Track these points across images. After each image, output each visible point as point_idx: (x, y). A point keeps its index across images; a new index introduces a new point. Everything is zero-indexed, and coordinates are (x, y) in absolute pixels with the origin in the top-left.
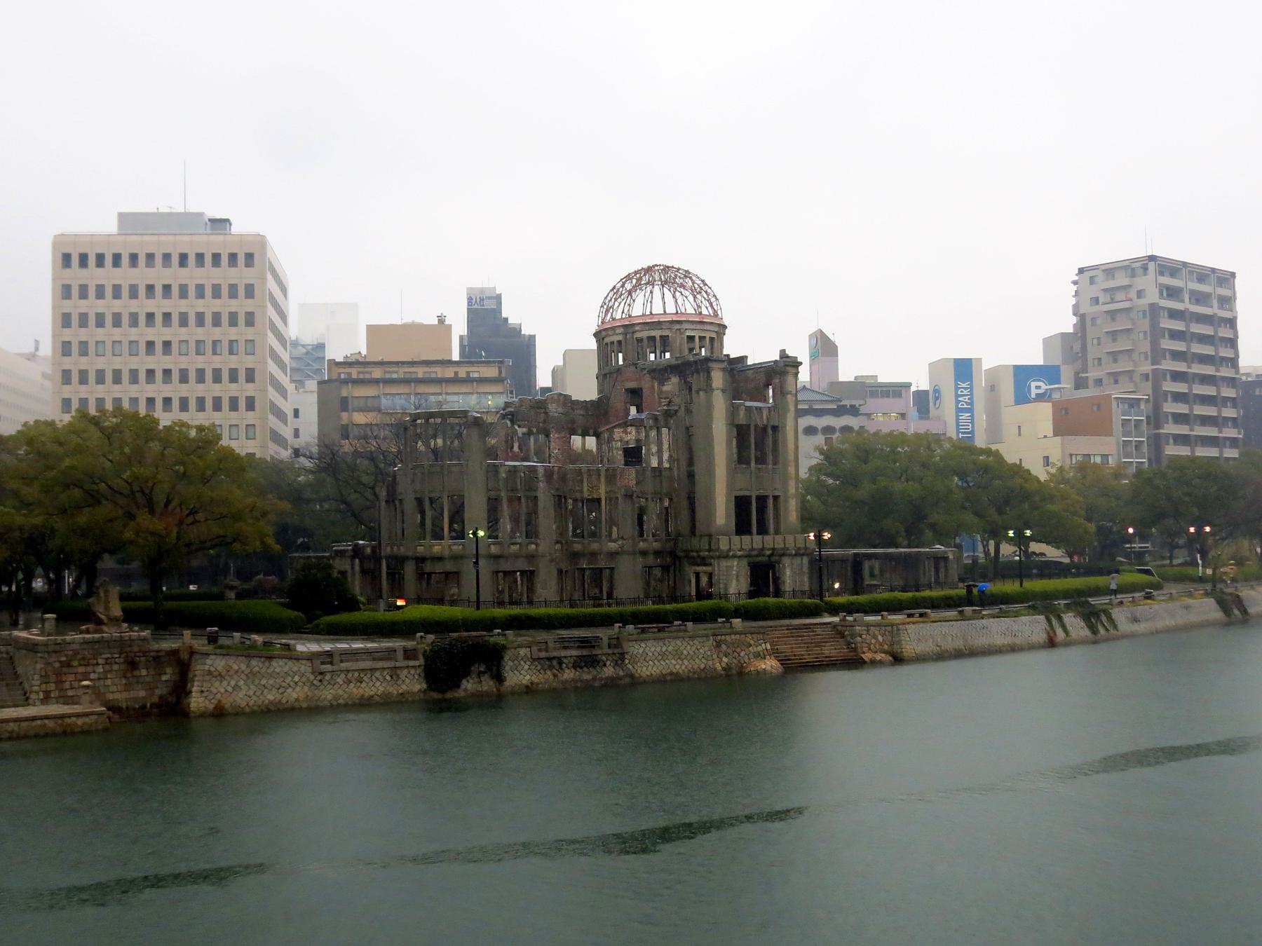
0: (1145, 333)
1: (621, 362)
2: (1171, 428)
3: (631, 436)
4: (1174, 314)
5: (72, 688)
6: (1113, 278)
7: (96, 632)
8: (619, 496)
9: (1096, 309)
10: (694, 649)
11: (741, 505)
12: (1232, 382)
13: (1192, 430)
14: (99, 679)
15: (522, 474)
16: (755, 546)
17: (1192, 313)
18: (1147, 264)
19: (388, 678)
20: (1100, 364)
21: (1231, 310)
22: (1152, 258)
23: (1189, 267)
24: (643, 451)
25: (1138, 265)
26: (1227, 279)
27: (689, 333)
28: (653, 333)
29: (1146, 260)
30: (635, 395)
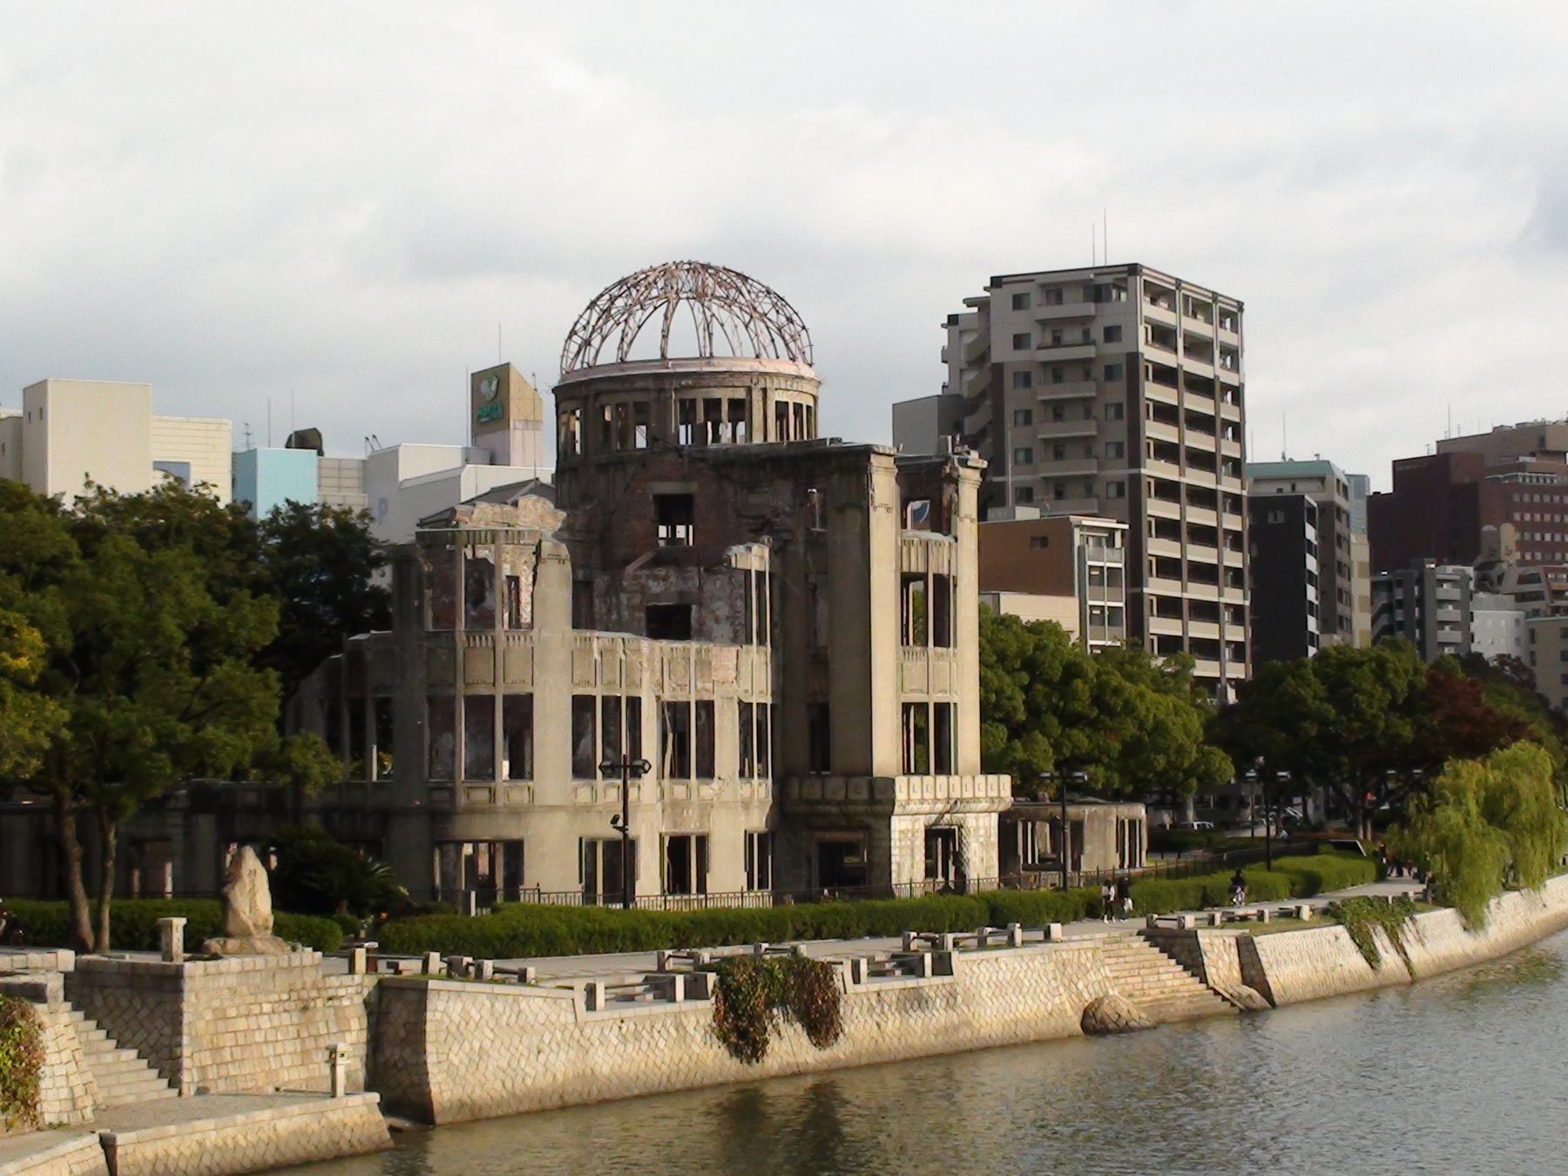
2: (1157, 587)
4: (1165, 375)
5: (233, 1061)
6: (1059, 300)
9: (1021, 356)
10: (1035, 976)
12: (1235, 503)
14: (266, 1042)
16: (939, 796)
19: (672, 1030)
20: (1029, 459)
22: (1133, 269)
23: (1184, 288)
24: (694, 614)
26: (1232, 315)
28: (717, 393)
29: (1124, 272)
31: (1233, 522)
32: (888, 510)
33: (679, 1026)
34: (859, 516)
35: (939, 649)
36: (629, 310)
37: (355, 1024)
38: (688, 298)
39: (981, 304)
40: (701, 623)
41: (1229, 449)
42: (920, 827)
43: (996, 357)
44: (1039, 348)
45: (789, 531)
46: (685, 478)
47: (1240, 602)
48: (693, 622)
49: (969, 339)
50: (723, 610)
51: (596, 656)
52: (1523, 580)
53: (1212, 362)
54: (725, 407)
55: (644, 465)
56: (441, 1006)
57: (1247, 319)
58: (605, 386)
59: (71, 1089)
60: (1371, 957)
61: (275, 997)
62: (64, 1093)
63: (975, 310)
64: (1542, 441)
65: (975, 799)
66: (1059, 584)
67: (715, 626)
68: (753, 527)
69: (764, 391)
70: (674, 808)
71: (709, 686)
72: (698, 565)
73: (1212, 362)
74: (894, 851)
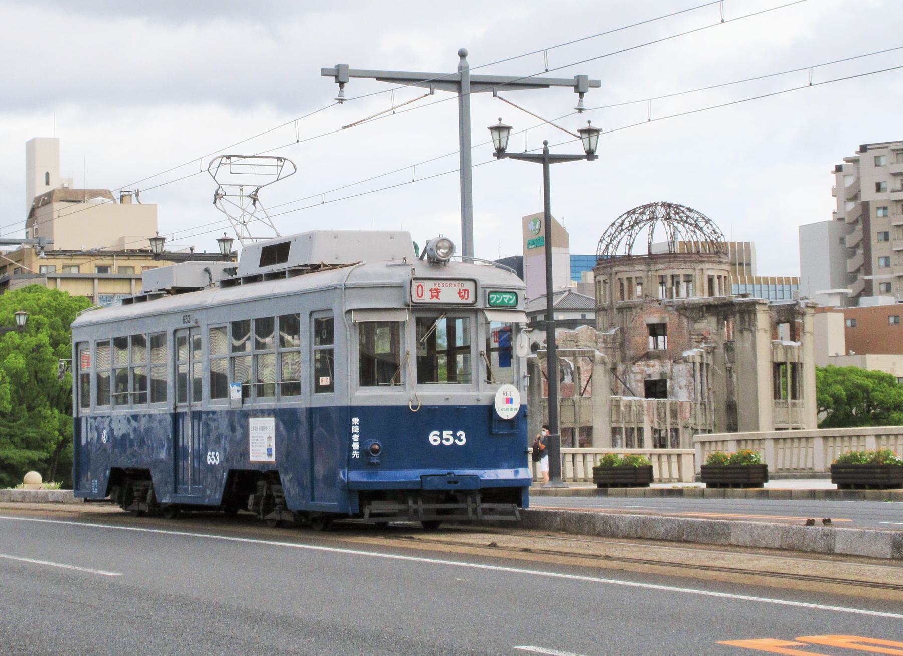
3: (654, 370)
9: (881, 196)
15: (634, 408)
20: (887, 265)
24: (668, 384)
27: (710, 272)
32: (765, 331)
34: (751, 335)
35: (794, 401)
38: (661, 220)
39: (856, 161)
43: (864, 198)
44: (893, 191)
45: (715, 342)
50: (683, 382)
67: (678, 389)
68: (697, 340)
72: (670, 359)
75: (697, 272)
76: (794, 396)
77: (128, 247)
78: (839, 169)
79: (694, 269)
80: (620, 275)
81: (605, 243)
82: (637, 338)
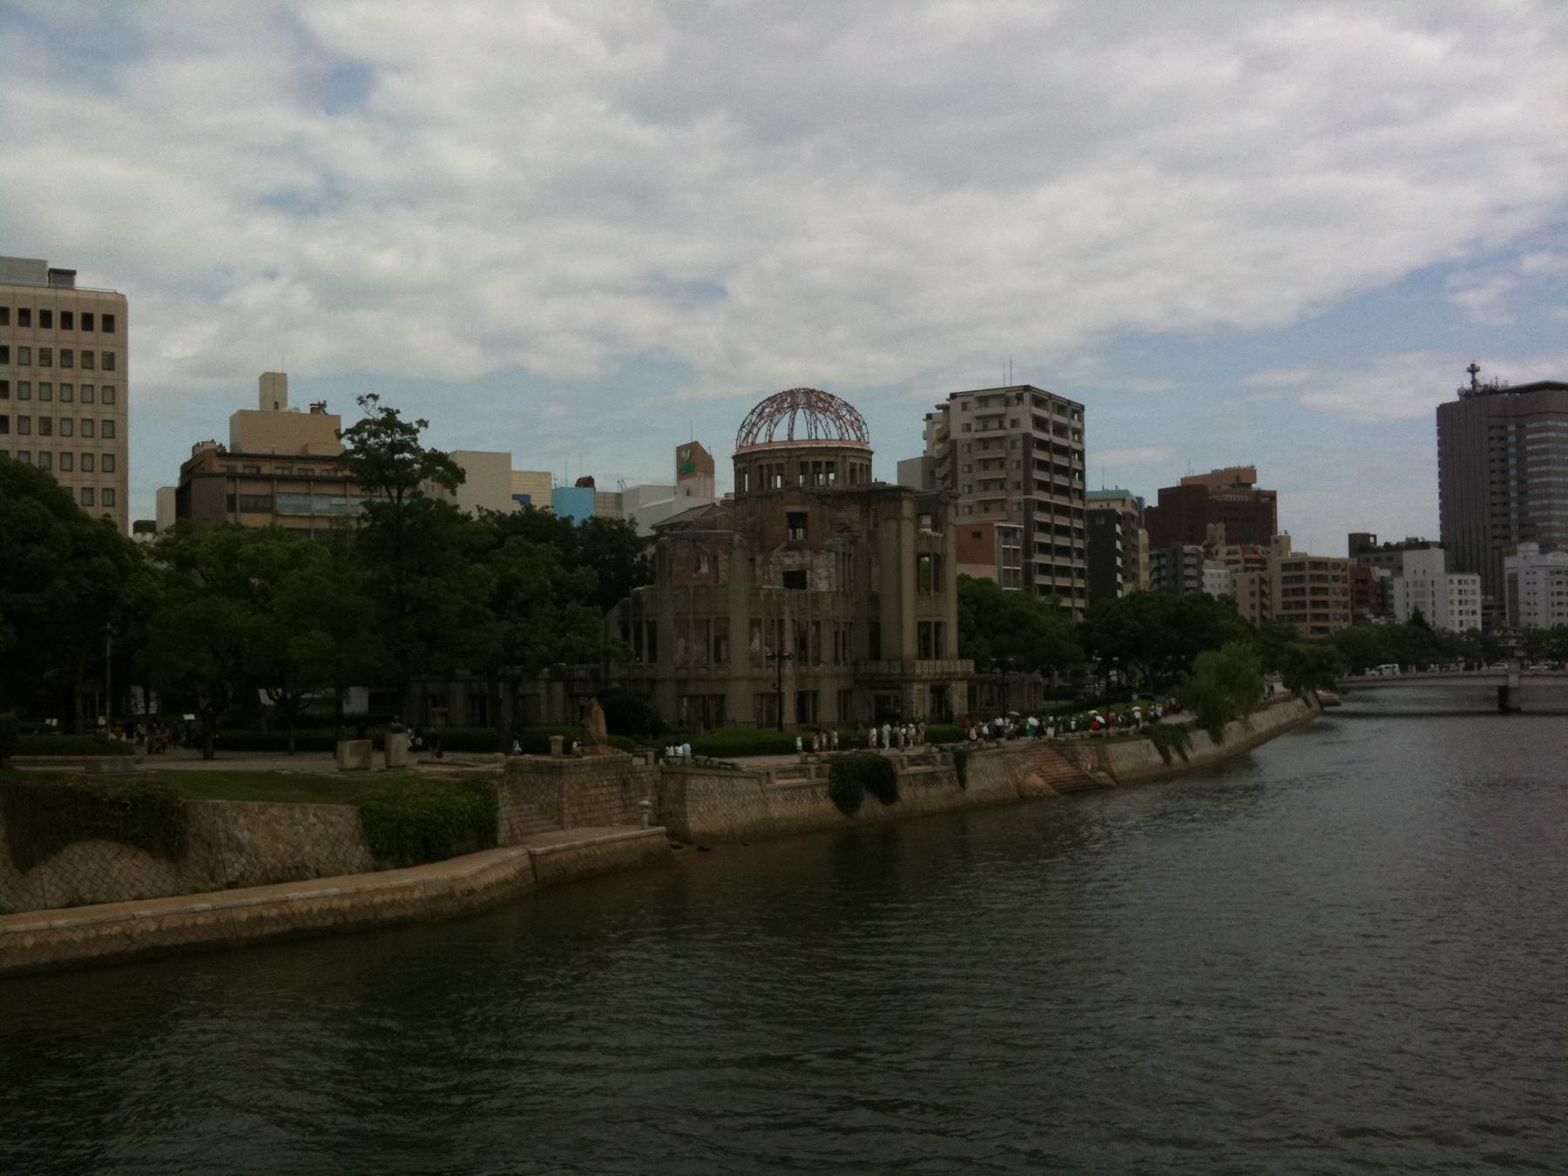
0: (1018, 462)
1: (779, 486)
3: (792, 561)
4: (1043, 445)
6: (987, 406)
7: (591, 753)
8: (820, 619)
9: (968, 435)
11: (923, 626)
12: (1079, 513)
13: (1053, 560)
17: (1055, 444)
18: (1021, 394)
21: (1080, 441)
22: (1027, 388)
24: (808, 576)
25: (1014, 394)
26: (1078, 410)
27: (853, 460)
28: (819, 459)
30: (796, 520)
31: (1078, 524)
33: (814, 793)
36: (771, 415)
37: (649, 791)
39: (945, 408)
40: (812, 580)
41: (1077, 485)
42: (928, 687)
43: (953, 436)
44: (976, 431)
46: (803, 504)
47: (1081, 566)
48: (808, 581)
49: (938, 426)
51: (762, 598)
52: (1229, 553)
53: (1067, 438)
54: (824, 466)
55: (782, 497)
56: (693, 781)
57: (1087, 414)
58: (761, 455)
59: (511, 826)
60: (1167, 758)
61: (609, 777)
62: (508, 828)
63: (941, 411)
64: (1238, 478)
65: (956, 673)
66: (988, 559)
67: (818, 581)
69: (844, 457)
70: (801, 678)
71: (817, 613)
72: (810, 549)
73: (1067, 438)
74: (914, 700)
75: (840, 459)
76: (936, 590)
77: (313, 452)
78: (929, 416)
79: (837, 456)
80: (759, 463)
81: (745, 430)
82: (777, 528)
